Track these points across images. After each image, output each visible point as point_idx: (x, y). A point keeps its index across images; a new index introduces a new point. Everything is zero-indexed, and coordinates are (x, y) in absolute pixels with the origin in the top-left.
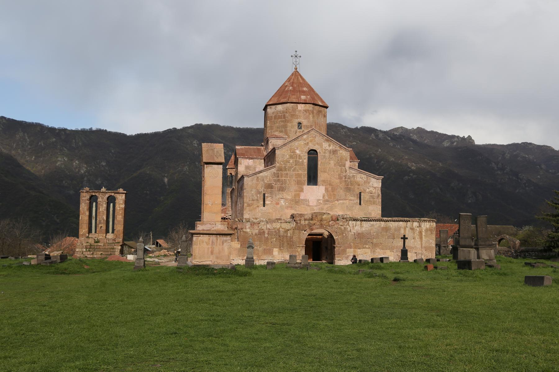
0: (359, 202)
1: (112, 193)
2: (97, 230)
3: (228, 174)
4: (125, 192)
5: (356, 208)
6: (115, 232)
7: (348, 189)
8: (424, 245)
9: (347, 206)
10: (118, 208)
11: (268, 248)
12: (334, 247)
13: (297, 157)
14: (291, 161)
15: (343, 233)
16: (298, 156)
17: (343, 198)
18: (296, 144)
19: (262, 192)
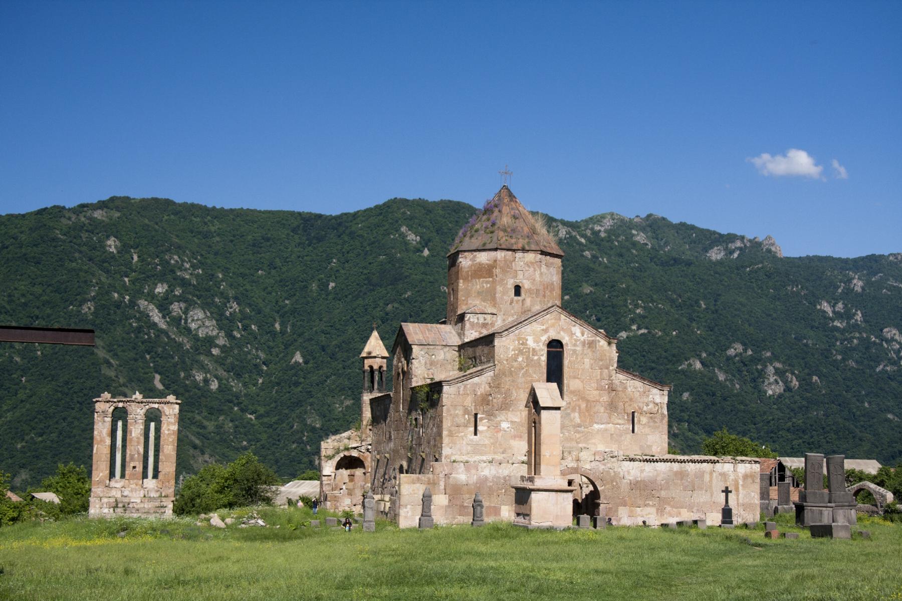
0: (631, 429)
1: (155, 403)
2: (127, 472)
3: (366, 367)
4: (179, 401)
5: (626, 438)
6: (161, 476)
7: (612, 407)
8: (741, 501)
9: (612, 435)
10: (167, 432)
11: (493, 505)
12: (598, 505)
13: (529, 352)
14: (520, 359)
15: (612, 481)
17: (606, 421)
18: (528, 330)
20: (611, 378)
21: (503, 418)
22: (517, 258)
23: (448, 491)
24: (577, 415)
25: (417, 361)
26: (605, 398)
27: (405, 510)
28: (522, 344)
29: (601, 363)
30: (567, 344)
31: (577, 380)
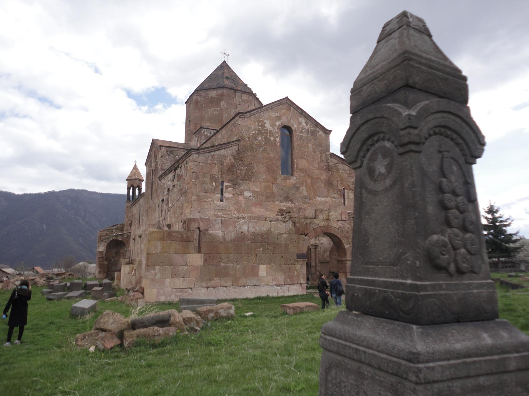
0: (343, 202)
7: (329, 184)
13: (267, 133)
14: (260, 138)
16: (268, 131)
17: (325, 195)
18: (266, 115)
19: (219, 178)
20: (328, 161)
21: (246, 187)
22: (237, 96)
23: (203, 249)
24: (304, 188)
25: (165, 158)
26: (324, 176)
27: (153, 272)
28: (261, 126)
29: (320, 149)
30: (296, 131)
31: (304, 160)
